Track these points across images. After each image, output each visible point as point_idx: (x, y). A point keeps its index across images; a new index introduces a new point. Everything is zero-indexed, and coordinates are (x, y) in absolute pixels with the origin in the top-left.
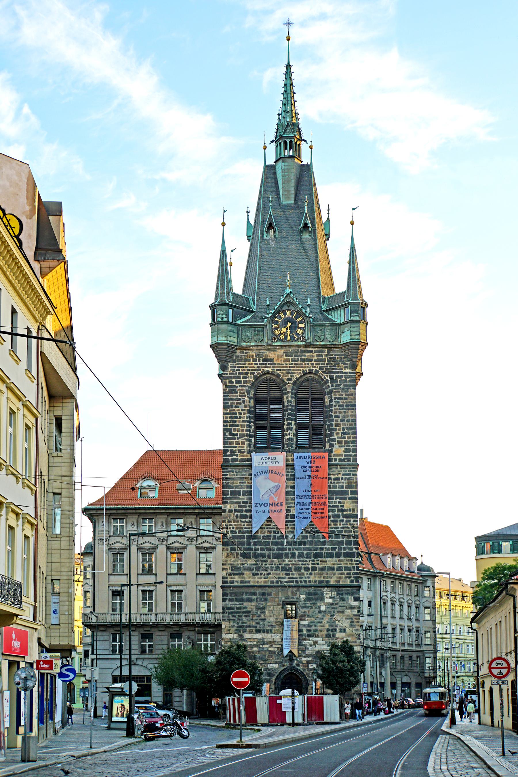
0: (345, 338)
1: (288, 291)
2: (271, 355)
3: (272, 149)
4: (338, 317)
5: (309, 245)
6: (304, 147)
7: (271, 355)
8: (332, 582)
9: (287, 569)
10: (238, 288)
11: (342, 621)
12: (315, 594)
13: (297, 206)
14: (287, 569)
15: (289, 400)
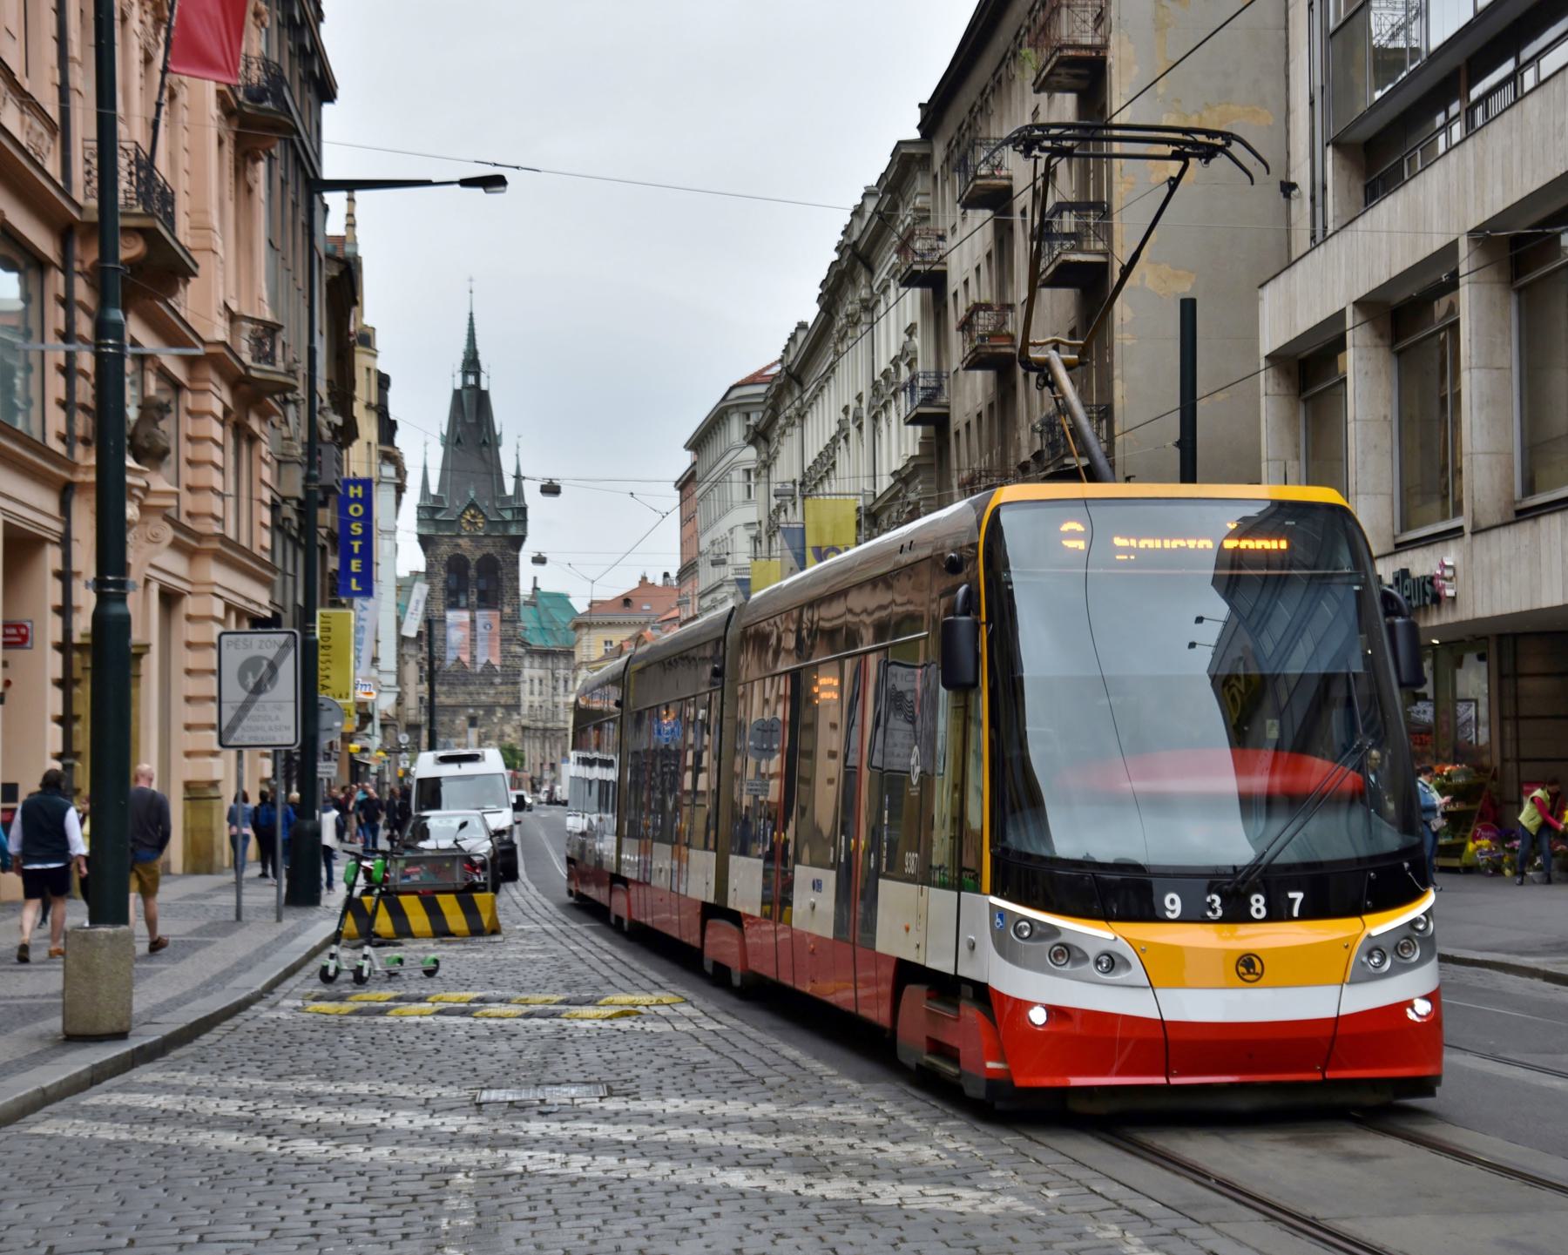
0: (513, 531)
1: (472, 494)
2: (460, 541)
3: (459, 377)
4: (508, 515)
5: (487, 455)
6: (483, 377)
7: (460, 541)
8: (502, 701)
9: (470, 694)
10: (434, 490)
11: (508, 729)
12: (490, 709)
13: (479, 425)
14: (470, 694)
15: (472, 573)
